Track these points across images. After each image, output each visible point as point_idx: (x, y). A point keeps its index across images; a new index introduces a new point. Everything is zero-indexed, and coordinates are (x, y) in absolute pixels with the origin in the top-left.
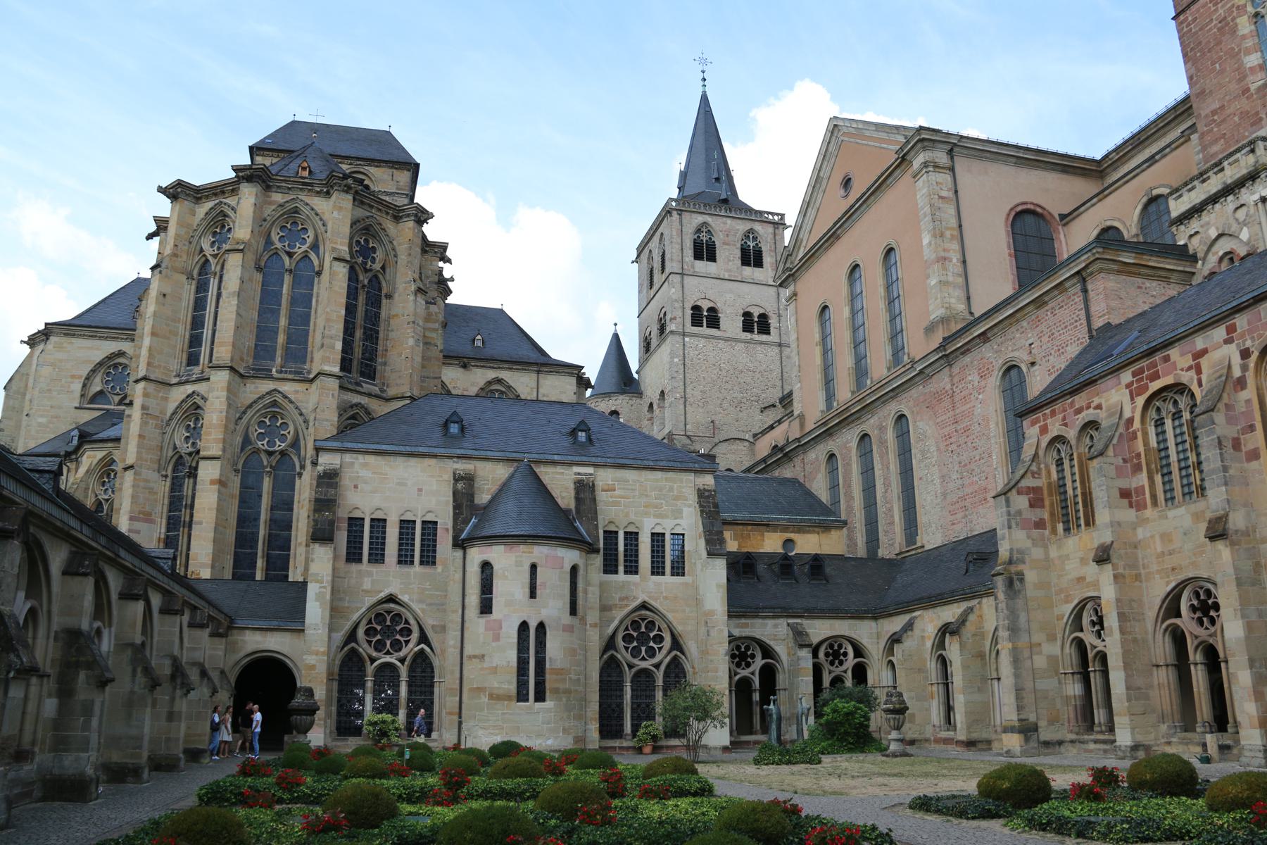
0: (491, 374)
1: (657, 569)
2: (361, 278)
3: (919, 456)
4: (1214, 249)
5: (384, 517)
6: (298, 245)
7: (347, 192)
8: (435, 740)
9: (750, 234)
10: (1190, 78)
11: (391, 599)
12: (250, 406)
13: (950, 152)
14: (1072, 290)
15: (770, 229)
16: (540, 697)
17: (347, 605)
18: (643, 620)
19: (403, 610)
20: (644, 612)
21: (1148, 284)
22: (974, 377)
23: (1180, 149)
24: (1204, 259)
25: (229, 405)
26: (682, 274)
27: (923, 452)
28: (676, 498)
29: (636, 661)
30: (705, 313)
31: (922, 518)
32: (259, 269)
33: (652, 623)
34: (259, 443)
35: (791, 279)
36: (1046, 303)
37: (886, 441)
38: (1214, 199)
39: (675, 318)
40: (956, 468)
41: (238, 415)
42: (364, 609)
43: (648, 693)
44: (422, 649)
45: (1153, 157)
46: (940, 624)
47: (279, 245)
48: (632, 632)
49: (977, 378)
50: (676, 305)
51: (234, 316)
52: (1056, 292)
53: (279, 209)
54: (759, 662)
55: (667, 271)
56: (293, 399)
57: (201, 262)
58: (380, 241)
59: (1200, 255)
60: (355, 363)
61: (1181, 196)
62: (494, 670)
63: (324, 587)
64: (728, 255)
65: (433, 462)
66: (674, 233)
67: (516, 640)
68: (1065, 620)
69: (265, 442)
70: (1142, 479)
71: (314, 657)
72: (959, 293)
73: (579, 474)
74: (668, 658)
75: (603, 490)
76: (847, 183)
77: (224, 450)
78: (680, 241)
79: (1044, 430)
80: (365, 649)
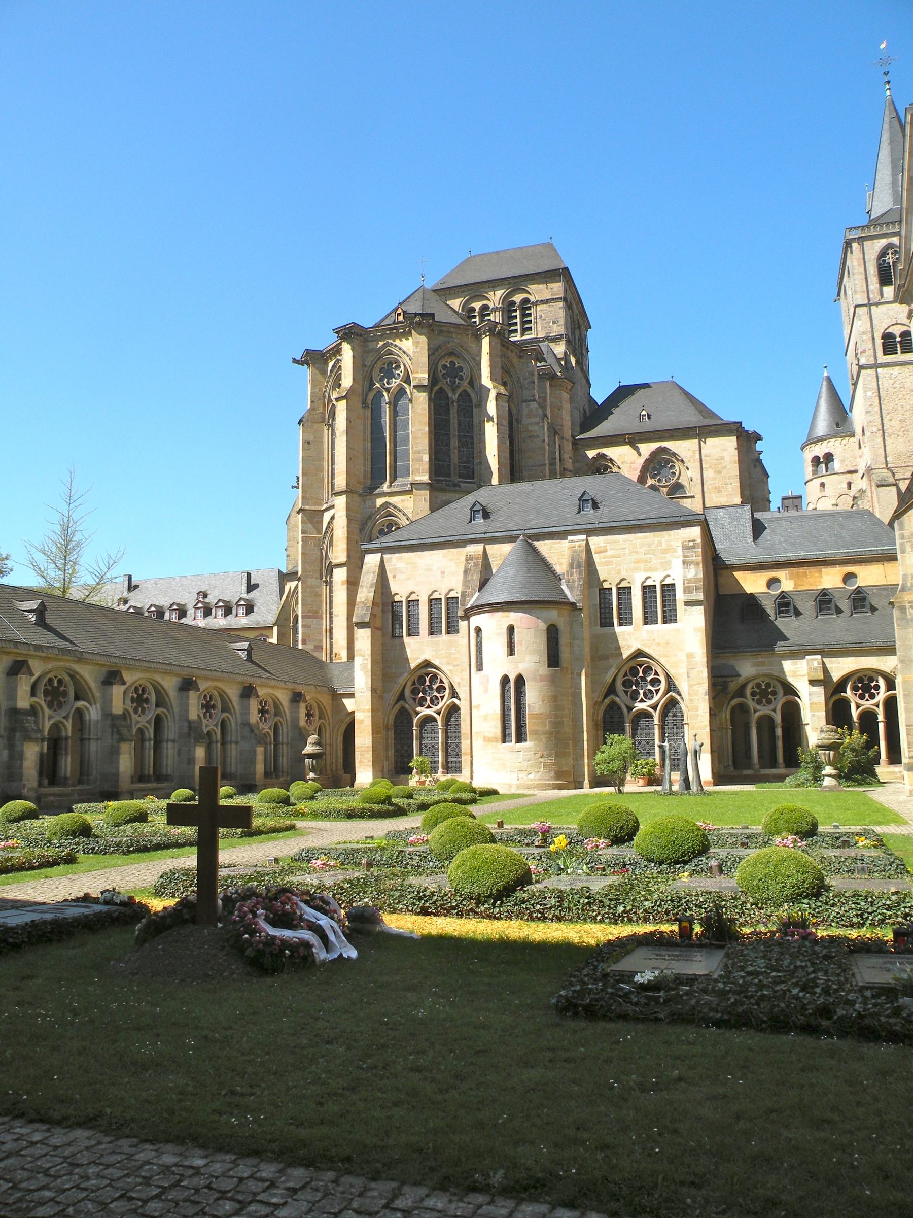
0: (654, 446)
1: (648, 619)
2: (450, 395)
16: (520, 738)
17: (393, 671)
28: (665, 551)
30: (898, 339)
33: (648, 669)
39: (864, 352)
43: (647, 731)
50: (865, 337)
54: (781, 700)
56: (401, 507)
60: (452, 468)
63: (366, 659)
73: (573, 541)
74: (664, 699)
75: (596, 553)
77: (349, 556)
78: (862, 270)
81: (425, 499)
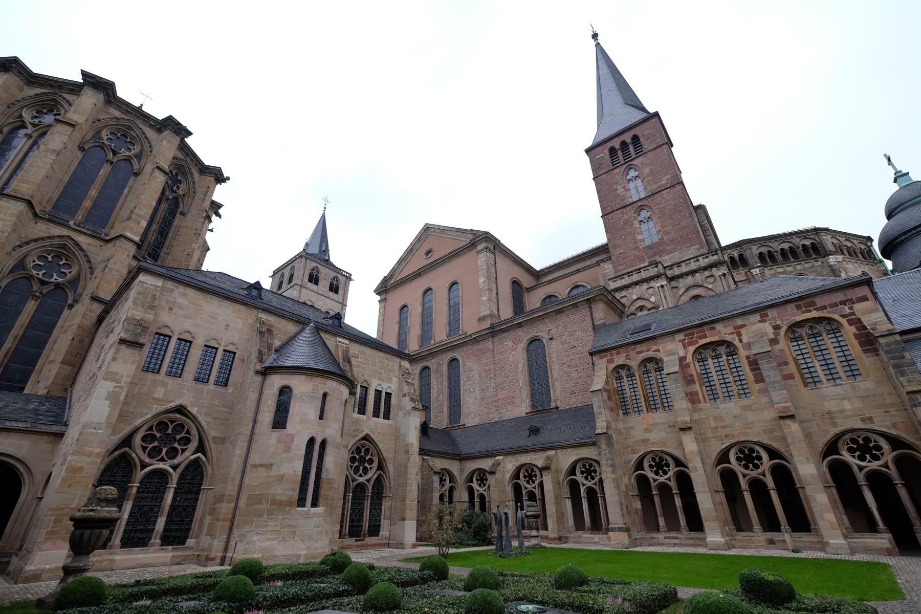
1: (376, 414)
2: (167, 193)
3: (465, 379)
4: (634, 304)
5: (191, 339)
6: (123, 150)
7: (177, 135)
8: (190, 548)
9: (335, 278)
10: (609, 240)
11: (181, 410)
12: (36, 240)
13: (494, 247)
14: (581, 307)
15: (344, 279)
16: (315, 504)
18: (363, 447)
19: (188, 421)
20: (364, 441)
21: (611, 311)
22: (509, 343)
23: (593, 268)
24: (629, 307)
25: (14, 231)
26: (301, 286)
27: (469, 379)
28: (390, 371)
29: (356, 477)
31: (464, 410)
32: (82, 149)
34: (34, 272)
35: (384, 292)
36: (563, 312)
37: (442, 371)
38: (636, 283)
40: (493, 386)
41: (18, 243)
42: (150, 416)
44: (199, 457)
45: (579, 270)
46: (518, 464)
47: (106, 143)
48: (356, 455)
49: (511, 343)
51: (48, 167)
52: (571, 307)
53: (115, 120)
55: (293, 283)
56: (84, 249)
57: (15, 125)
58: (187, 179)
59: (627, 305)
61: (616, 280)
62: (280, 479)
64: (324, 285)
65: (242, 308)
66: (302, 267)
67: (304, 453)
68: (632, 463)
69: (41, 273)
70: (697, 387)
71: (85, 458)
72: (495, 306)
73: (340, 342)
74: (376, 476)
76: (429, 252)
79: (611, 361)
80: (138, 453)
81: (128, 255)
